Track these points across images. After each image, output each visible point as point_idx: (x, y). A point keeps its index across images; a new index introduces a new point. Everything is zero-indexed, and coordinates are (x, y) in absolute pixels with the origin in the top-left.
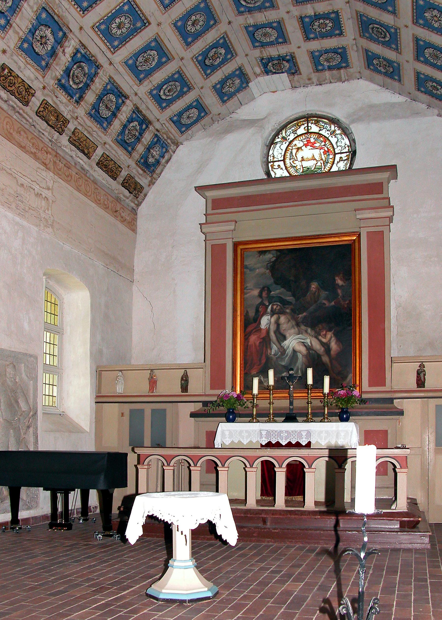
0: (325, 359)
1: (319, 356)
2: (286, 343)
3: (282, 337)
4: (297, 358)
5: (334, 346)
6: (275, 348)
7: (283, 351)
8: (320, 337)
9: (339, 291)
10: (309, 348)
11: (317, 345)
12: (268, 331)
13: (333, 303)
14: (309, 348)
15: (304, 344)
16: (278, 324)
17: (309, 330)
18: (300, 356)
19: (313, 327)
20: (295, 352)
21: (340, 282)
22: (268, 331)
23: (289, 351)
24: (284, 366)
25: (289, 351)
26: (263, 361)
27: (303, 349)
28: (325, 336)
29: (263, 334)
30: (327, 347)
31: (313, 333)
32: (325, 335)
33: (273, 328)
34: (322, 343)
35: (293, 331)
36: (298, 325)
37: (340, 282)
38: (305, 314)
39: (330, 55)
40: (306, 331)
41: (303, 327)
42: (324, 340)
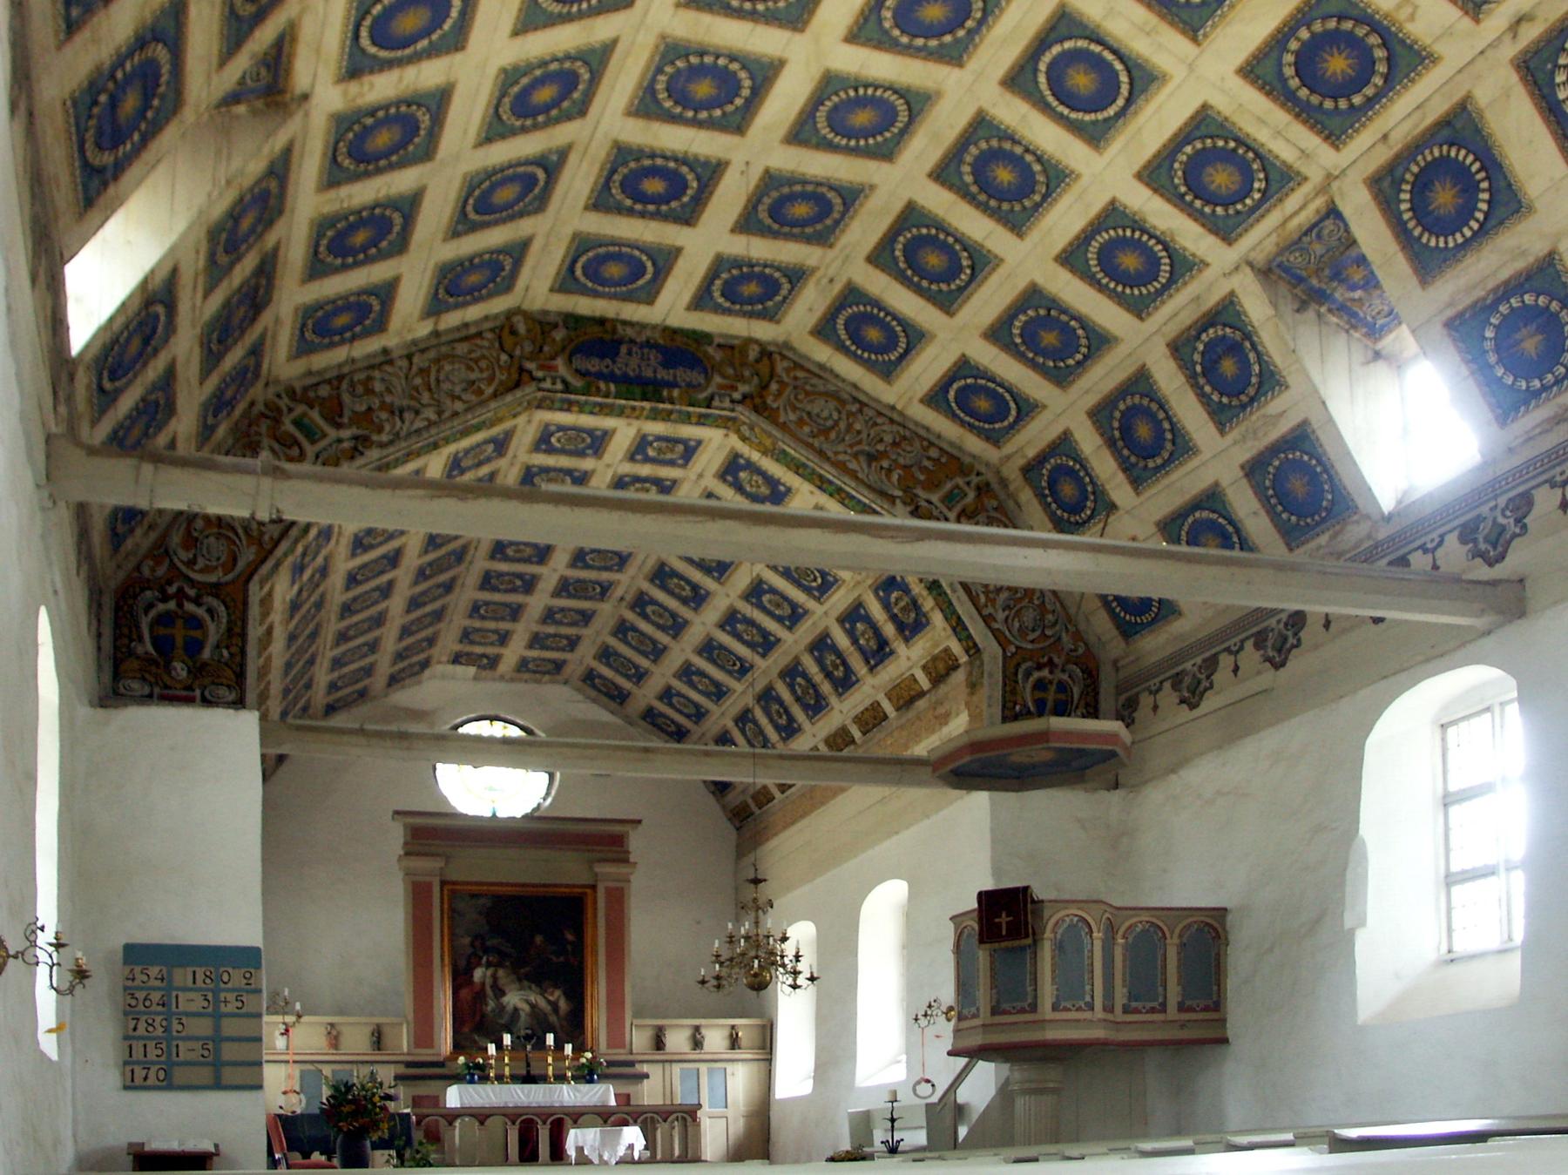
0: (553, 1019)
2: (505, 1000)
3: (500, 992)
4: (519, 1016)
5: (563, 1005)
6: (491, 1004)
7: (502, 1008)
10: (533, 1006)
11: (542, 1003)
12: (483, 984)
13: (562, 959)
14: (533, 1006)
15: (527, 1002)
16: (494, 977)
17: (533, 986)
18: (522, 1014)
19: (539, 983)
20: (516, 1010)
22: (483, 984)
23: (510, 1008)
24: (503, 1025)
25: (510, 1008)
26: (478, 1018)
27: (526, 1008)
29: (477, 988)
30: (555, 1006)
31: (538, 990)
33: (489, 981)
34: (549, 1002)
35: (513, 986)
36: (520, 980)
38: (527, 969)
40: (530, 988)
41: (526, 983)
42: (551, 998)
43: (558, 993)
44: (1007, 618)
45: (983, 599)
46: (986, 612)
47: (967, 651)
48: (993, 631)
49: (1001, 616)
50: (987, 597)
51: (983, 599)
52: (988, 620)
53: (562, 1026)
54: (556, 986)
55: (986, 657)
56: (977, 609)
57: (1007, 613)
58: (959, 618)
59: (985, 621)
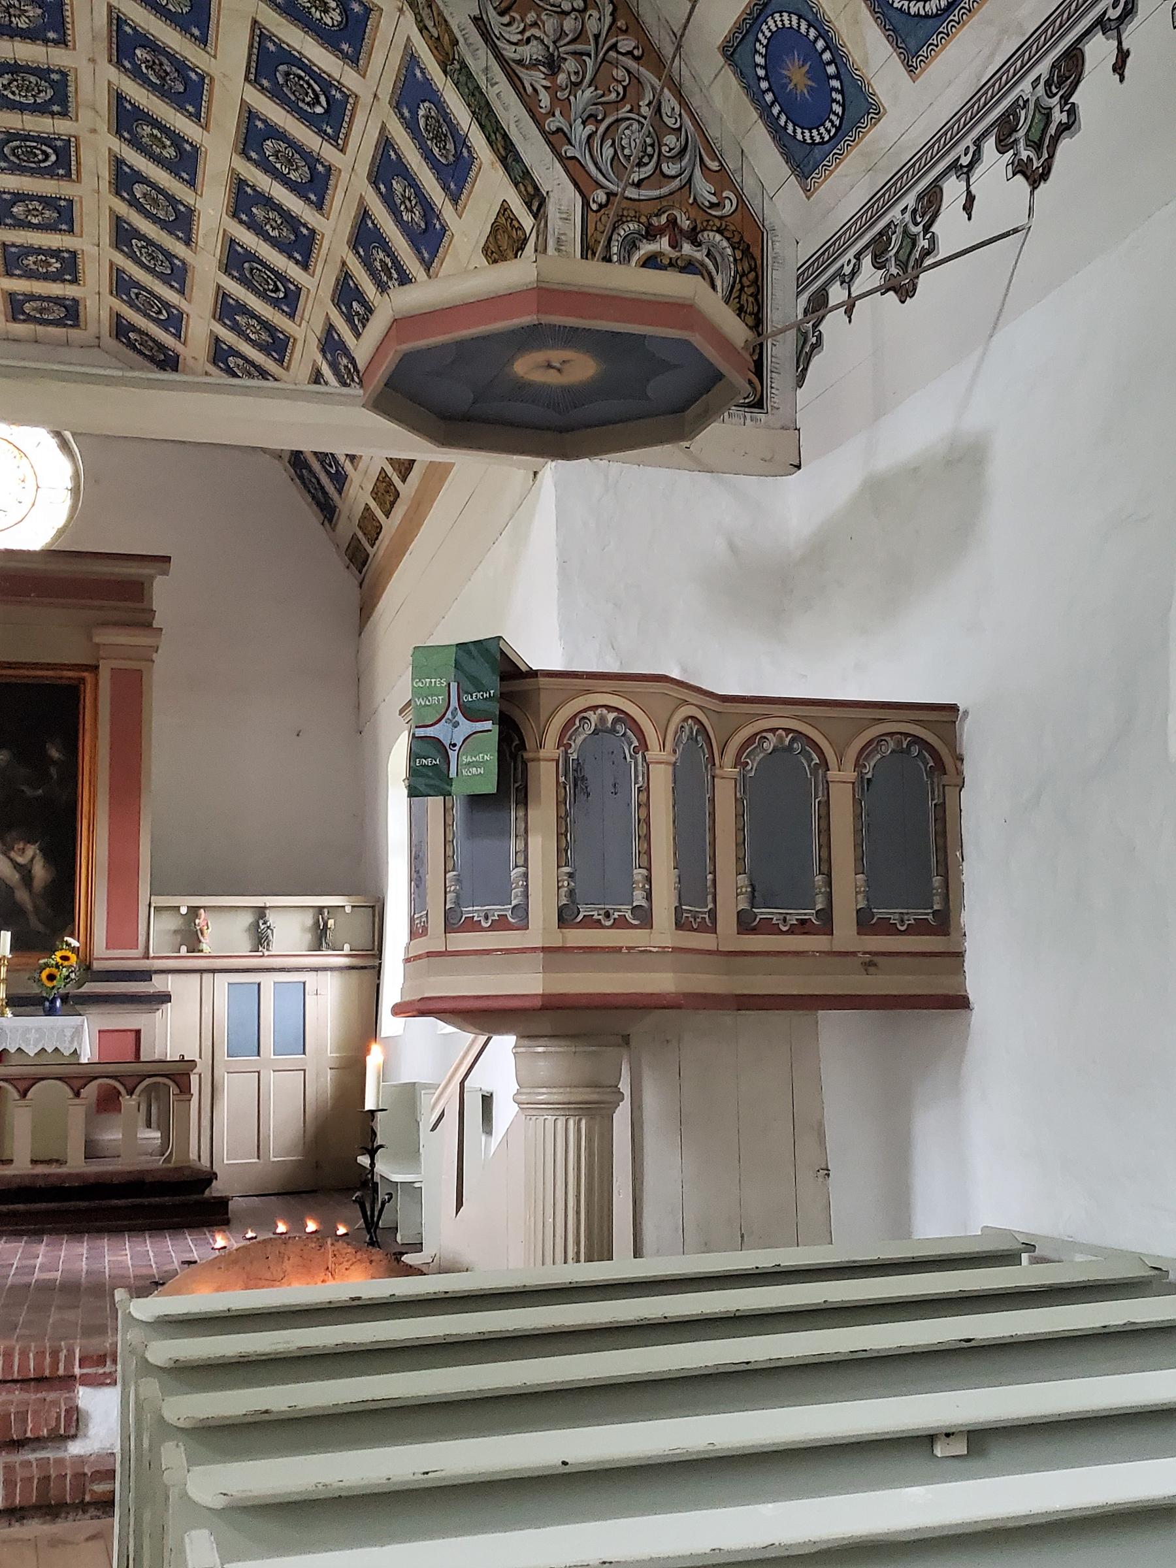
0: (22, 895)
1: (10, 890)
5: (40, 871)
8: (12, 854)
9: (53, 771)
21: (54, 753)
28: (23, 853)
32: (23, 850)
34: (17, 866)
37: (54, 753)
39: (45, 304)
42: (20, 860)
43: (31, 850)
44: (590, 137)
45: (545, 99)
46: (552, 124)
47: (529, 205)
48: (561, 159)
49: (580, 132)
50: (554, 99)
51: (545, 99)
52: (555, 140)
53: (35, 907)
54: (30, 841)
55: (551, 209)
56: (533, 117)
57: (590, 128)
58: (505, 136)
59: (549, 143)
